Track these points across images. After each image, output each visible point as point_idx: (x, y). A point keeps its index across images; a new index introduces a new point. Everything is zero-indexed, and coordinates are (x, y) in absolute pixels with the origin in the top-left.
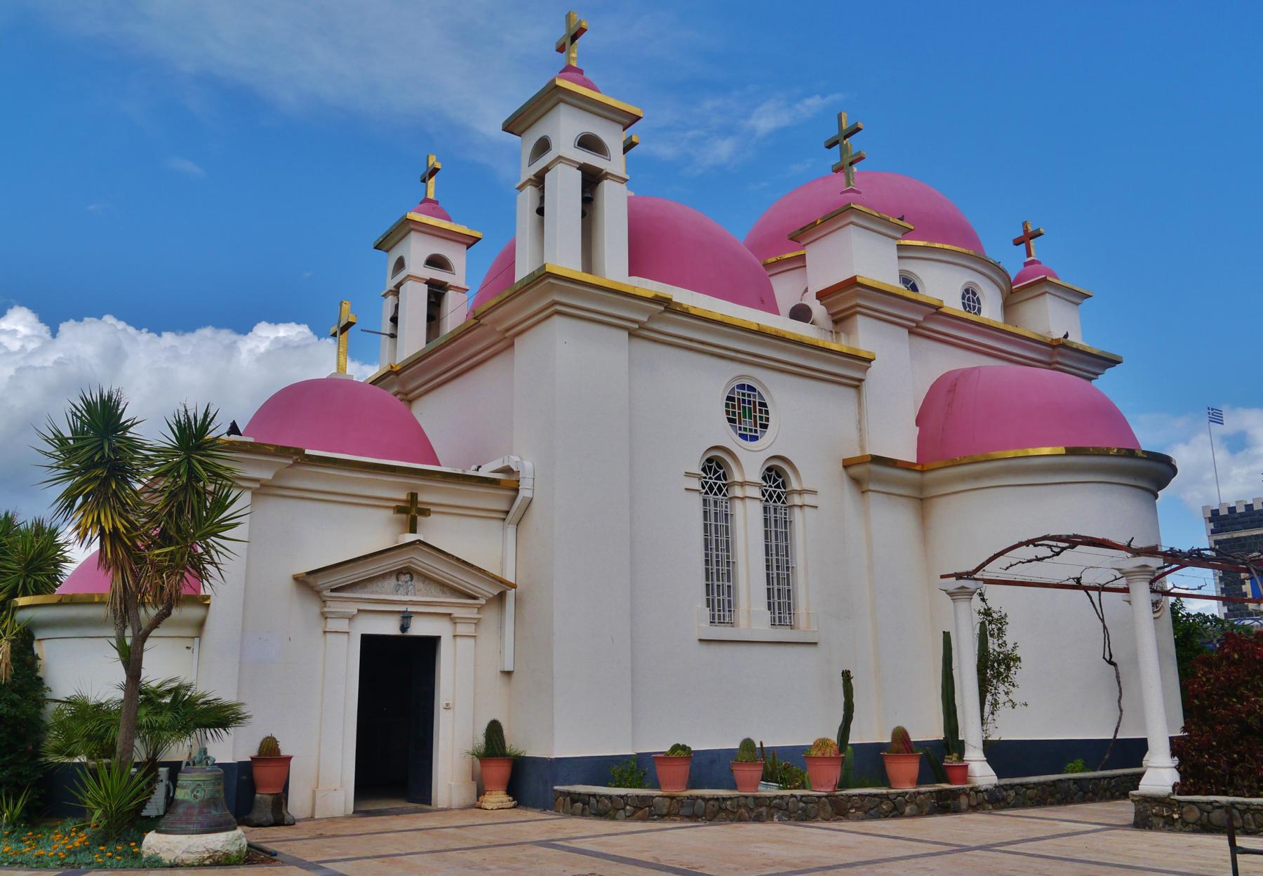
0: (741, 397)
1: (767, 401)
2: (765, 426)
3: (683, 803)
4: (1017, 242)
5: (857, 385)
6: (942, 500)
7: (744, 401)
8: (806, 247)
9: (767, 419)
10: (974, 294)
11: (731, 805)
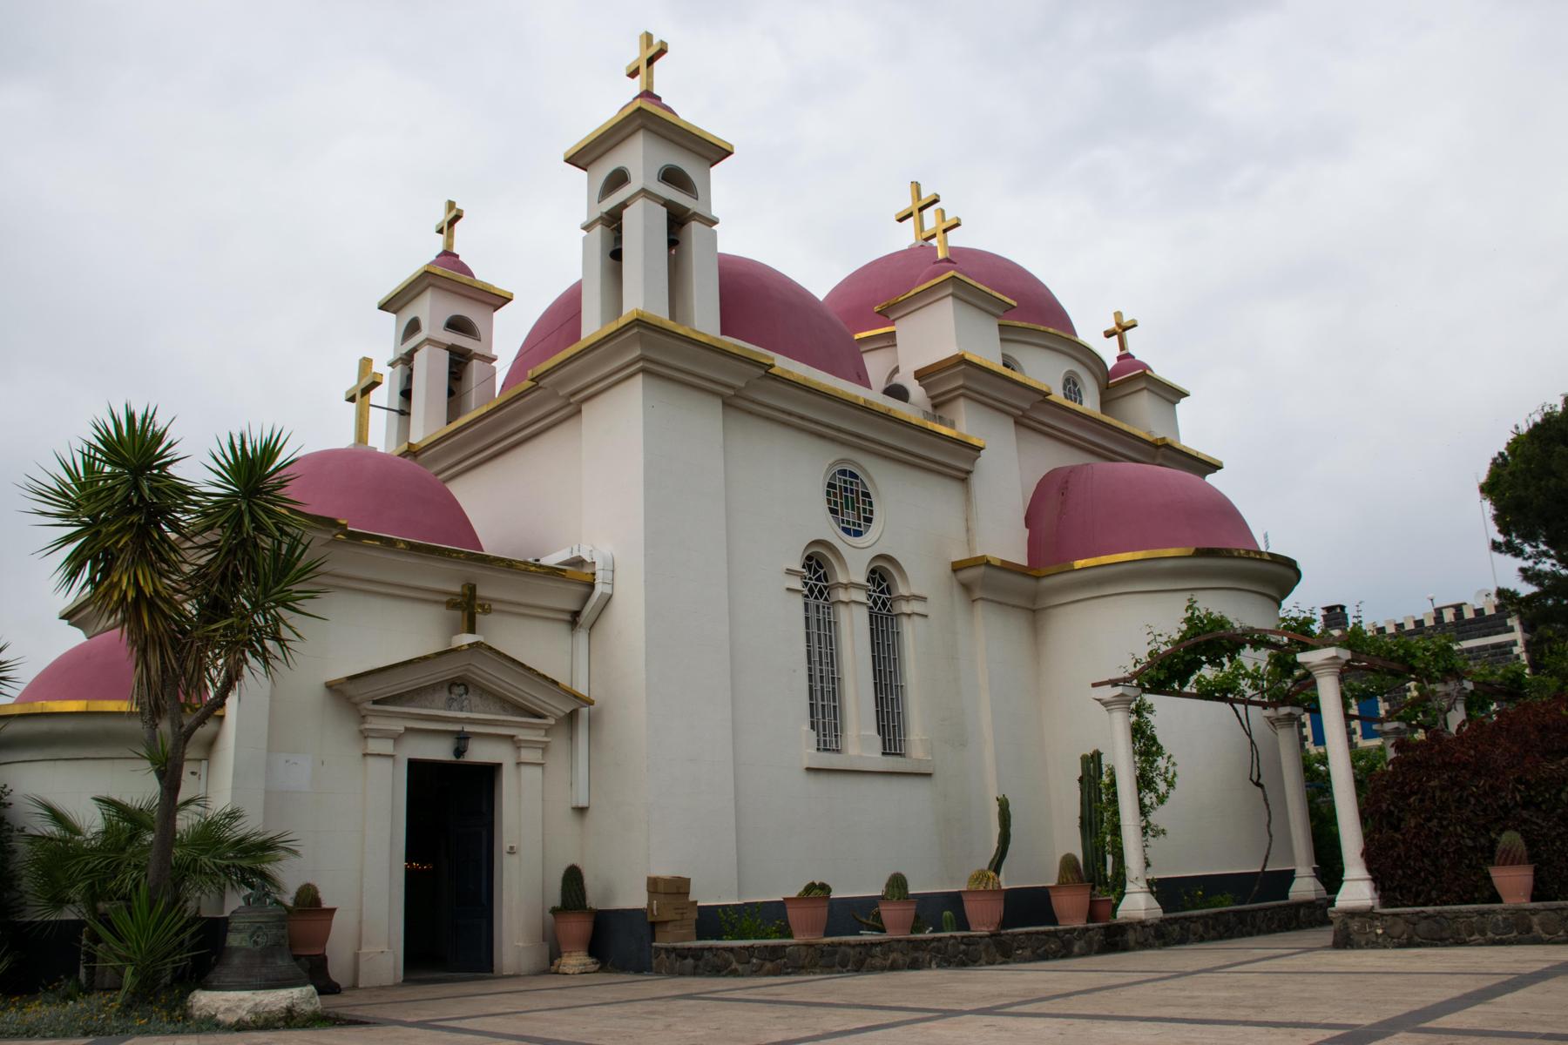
0: (843, 485)
1: (871, 491)
2: (869, 520)
3: (823, 951)
4: (1108, 334)
5: (963, 478)
6: (1061, 609)
7: (846, 489)
8: (896, 322)
9: (871, 512)
10: (1075, 385)
11: (881, 951)
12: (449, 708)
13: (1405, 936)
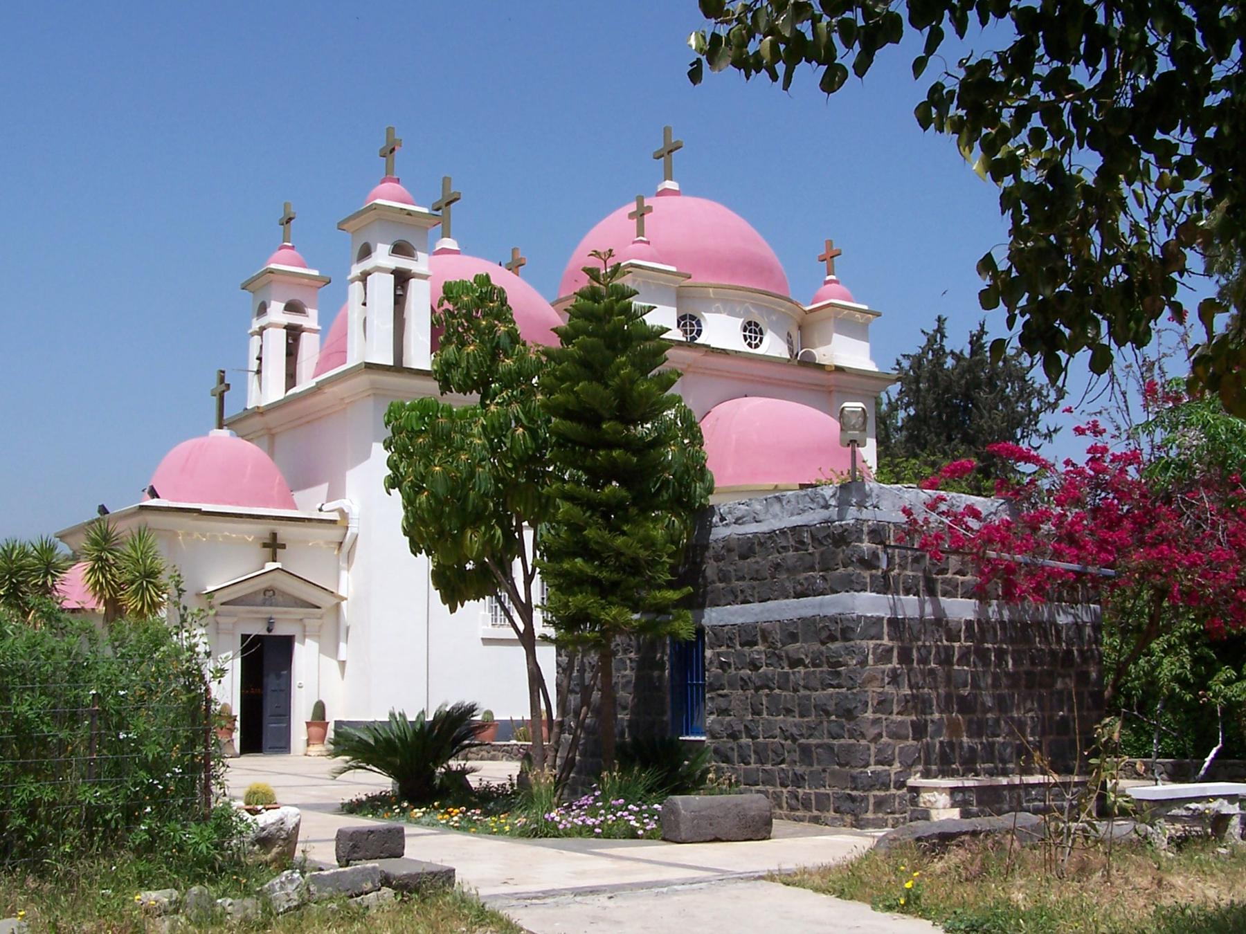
10: (756, 325)
12: (264, 604)
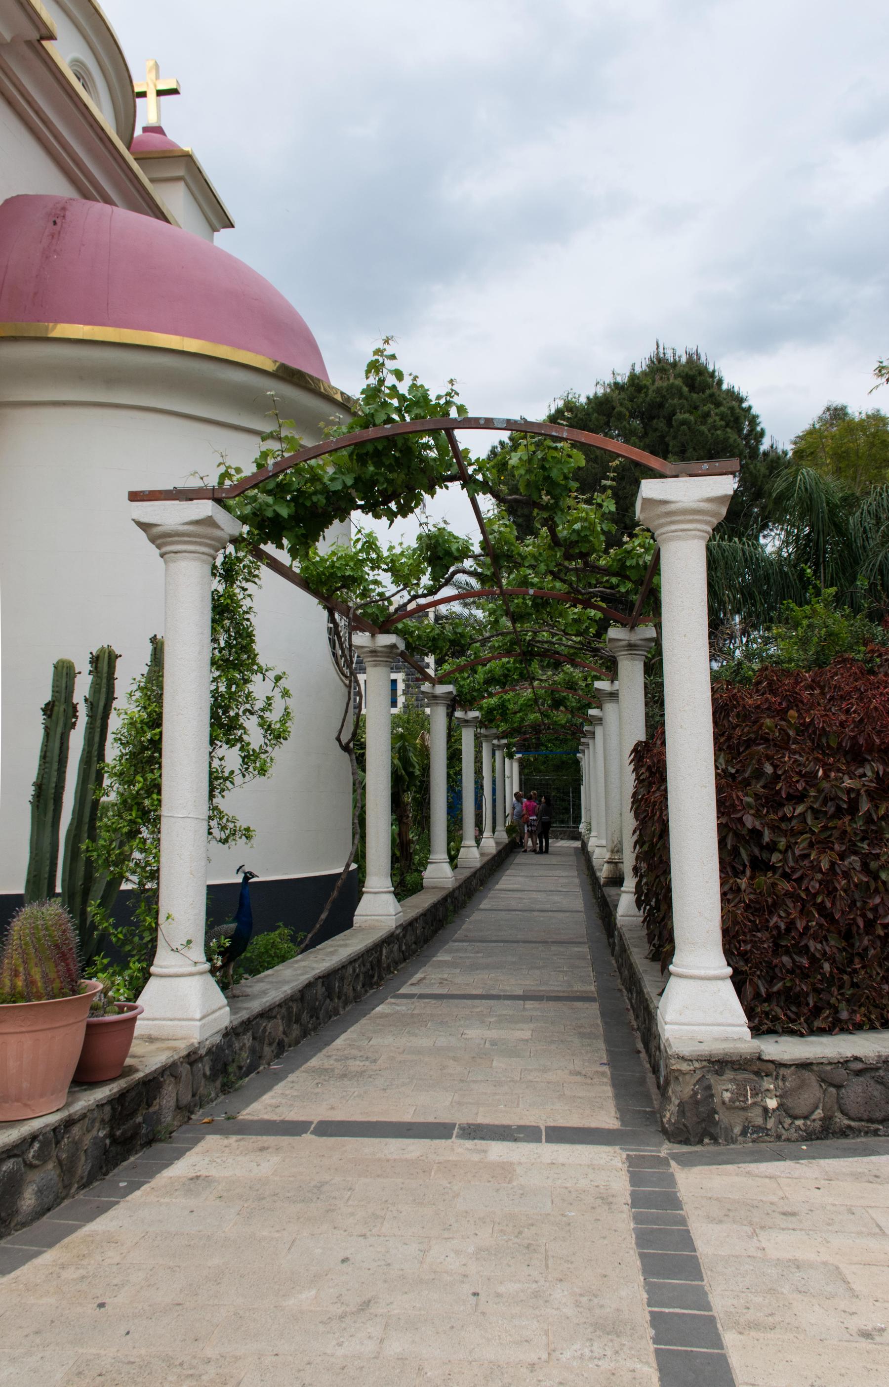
13: (819, 1113)
